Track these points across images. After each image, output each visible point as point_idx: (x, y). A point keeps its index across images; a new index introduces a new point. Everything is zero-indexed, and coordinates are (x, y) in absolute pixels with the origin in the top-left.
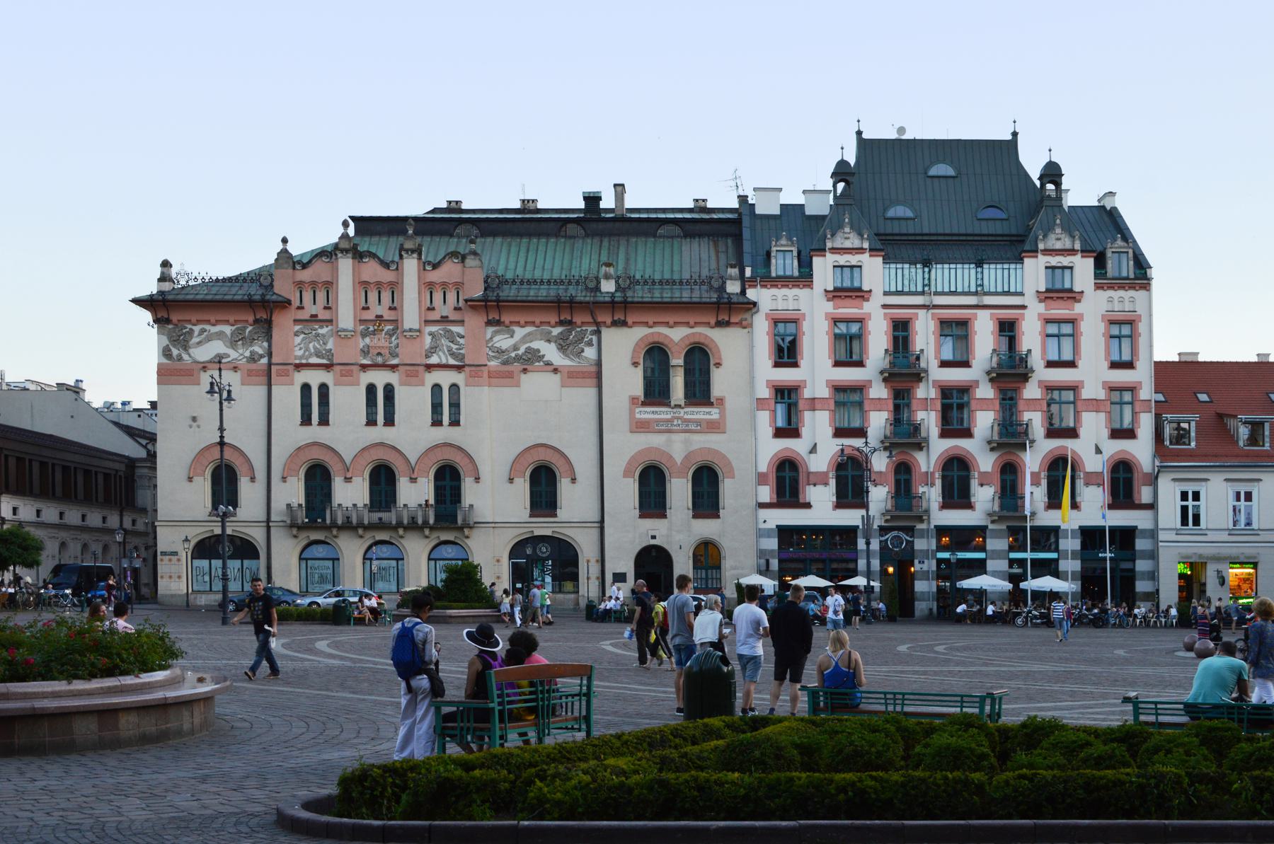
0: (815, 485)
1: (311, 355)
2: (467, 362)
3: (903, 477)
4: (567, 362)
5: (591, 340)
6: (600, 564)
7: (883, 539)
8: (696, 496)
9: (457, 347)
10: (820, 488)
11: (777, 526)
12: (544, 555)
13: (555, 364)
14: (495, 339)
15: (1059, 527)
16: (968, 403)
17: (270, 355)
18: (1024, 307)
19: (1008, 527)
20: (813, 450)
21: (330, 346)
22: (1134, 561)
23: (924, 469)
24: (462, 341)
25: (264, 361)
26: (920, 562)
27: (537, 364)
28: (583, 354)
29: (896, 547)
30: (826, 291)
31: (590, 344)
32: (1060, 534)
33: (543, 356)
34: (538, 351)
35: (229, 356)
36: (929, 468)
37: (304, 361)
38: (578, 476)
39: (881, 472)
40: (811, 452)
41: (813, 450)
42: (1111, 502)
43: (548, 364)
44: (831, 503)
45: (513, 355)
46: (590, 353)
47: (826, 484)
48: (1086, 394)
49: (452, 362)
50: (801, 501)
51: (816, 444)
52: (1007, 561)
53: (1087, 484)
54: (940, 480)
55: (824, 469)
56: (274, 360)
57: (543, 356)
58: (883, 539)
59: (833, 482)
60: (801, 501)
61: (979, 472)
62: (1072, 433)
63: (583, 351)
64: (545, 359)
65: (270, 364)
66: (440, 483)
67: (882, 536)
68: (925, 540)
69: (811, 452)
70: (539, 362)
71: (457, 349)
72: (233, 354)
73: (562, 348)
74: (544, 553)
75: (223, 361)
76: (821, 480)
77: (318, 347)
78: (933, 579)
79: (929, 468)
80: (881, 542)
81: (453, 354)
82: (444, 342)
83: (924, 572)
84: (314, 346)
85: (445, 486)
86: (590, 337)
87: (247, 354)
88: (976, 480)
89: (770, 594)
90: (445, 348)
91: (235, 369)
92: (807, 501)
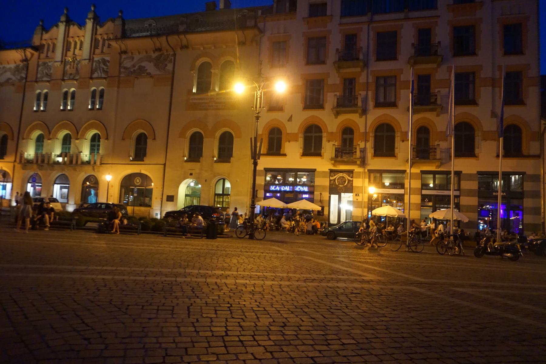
0: (289, 142)
1: (42, 77)
2: (109, 75)
3: (348, 136)
4: (158, 73)
5: (171, 59)
6: (162, 189)
7: (331, 178)
8: (221, 150)
9: (107, 67)
10: (293, 144)
11: (265, 169)
12: (136, 184)
13: (152, 74)
14: (125, 62)
15: (461, 172)
16: (395, 85)
17: (26, 78)
18: (439, 16)
19: (421, 171)
20: (290, 119)
21: (51, 72)
22: (522, 198)
23: (362, 130)
24: (108, 64)
25: (24, 81)
26: (356, 195)
27: (143, 74)
28: (167, 68)
29: (341, 185)
30: (303, 18)
31: (170, 62)
32: (462, 177)
33: (147, 70)
34: (144, 67)
35: (10, 79)
36: (366, 129)
37: (40, 80)
38: (157, 137)
39: (332, 133)
40: (289, 121)
41: (290, 119)
42: (504, 154)
43: (149, 74)
44: (299, 154)
45: (132, 70)
46: (170, 67)
47: (297, 141)
48: (486, 73)
49: (103, 76)
50: (282, 153)
51: (292, 115)
52: (420, 196)
53: (485, 139)
54: (373, 139)
55: (296, 132)
56: (28, 79)
57: (147, 70)
58: (331, 178)
59: (301, 141)
60: (282, 153)
61: (402, 132)
62: (474, 103)
63: (166, 65)
64: (148, 71)
65: (26, 81)
66: (93, 143)
67: (332, 177)
68: (360, 180)
69: (289, 121)
70: (144, 73)
71: (107, 69)
72: (14, 78)
73: (155, 65)
74: (138, 183)
75: (10, 81)
76: (293, 138)
77: (47, 71)
78: (364, 208)
79: (366, 129)
80: (330, 180)
81: (104, 71)
82: (102, 65)
83: (359, 202)
84: (46, 73)
85: (95, 145)
86: (171, 58)
87: (19, 78)
88: (399, 138)
89: (257, 213)
90: (101, 69)
91: (13, 85)
92: (285, 153)
